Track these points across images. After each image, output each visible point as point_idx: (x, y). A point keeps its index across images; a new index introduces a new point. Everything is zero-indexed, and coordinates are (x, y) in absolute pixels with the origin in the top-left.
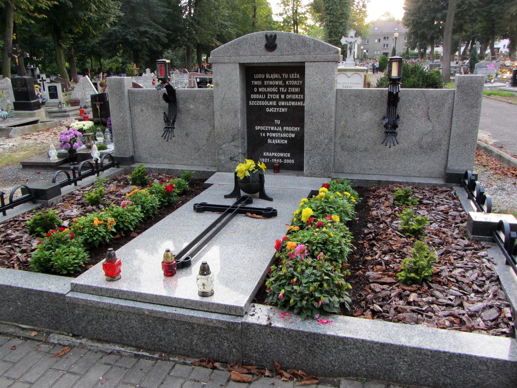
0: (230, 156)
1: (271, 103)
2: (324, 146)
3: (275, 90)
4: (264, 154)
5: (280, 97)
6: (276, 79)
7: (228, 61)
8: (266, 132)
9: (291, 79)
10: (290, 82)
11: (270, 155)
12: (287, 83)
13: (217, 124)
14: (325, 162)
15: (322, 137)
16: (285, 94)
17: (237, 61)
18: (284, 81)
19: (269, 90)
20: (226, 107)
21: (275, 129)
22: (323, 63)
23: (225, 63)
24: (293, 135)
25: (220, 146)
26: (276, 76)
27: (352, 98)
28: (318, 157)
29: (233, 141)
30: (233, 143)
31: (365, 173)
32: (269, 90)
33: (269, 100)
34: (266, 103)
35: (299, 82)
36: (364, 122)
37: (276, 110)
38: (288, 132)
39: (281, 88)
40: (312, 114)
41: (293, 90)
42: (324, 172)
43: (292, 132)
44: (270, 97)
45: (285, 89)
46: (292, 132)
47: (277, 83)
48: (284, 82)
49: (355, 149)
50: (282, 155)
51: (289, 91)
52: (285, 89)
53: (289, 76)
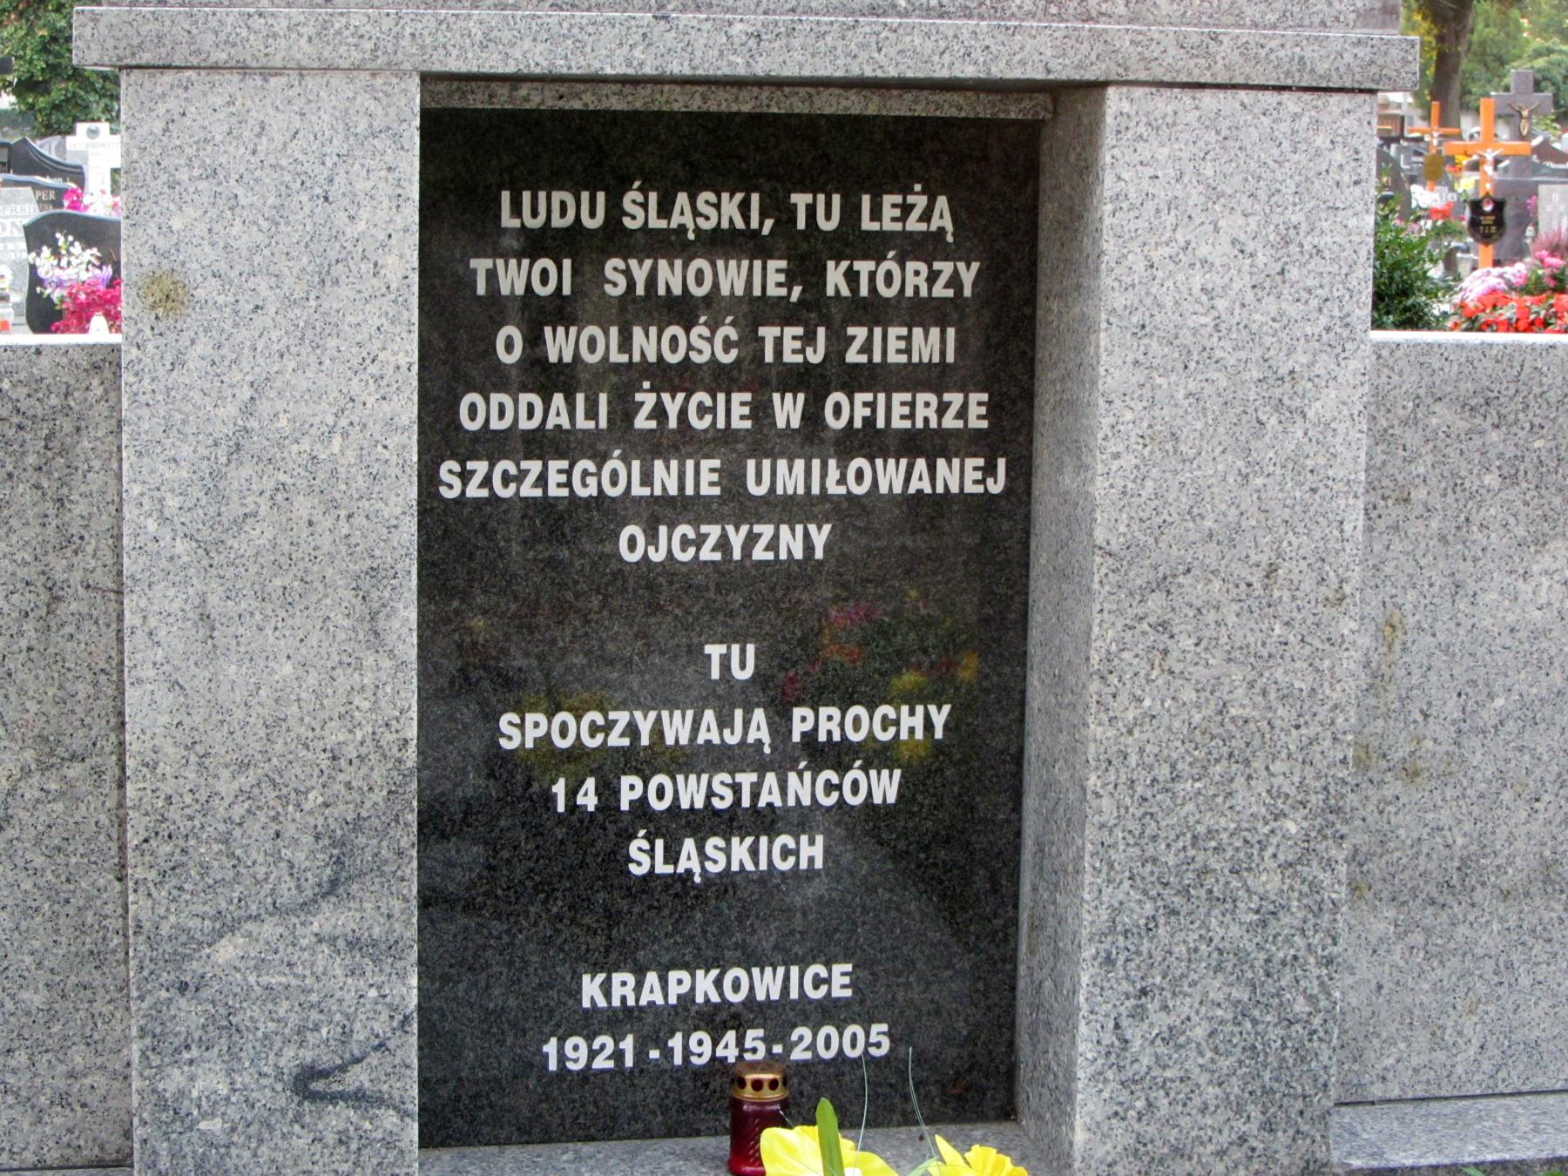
0: (291, 1058)
1: (666, 477)
2: (1269, 881)
3: (708, 344)
4: (591, 989)
5: (761, 412)
6: (720, 243)
7: (304, 51)
8: (607, 767)
9: (875, 246)
10: (864, 267)
11: (652, 992)
12: (835, 277)
13: (148, 710)
14: (1275, 1034)
15: (1249, 800)
16: (813, 383)
17: (413, 58)
18: (806, 260)
19: (646, 344)
20: (259, 534)
21: (710, 732)
22: (1270, 98)
23: (267, 72)
24: (885, 787)
25: (178, 960)
26: (724, 210)
27: (1443, 416)
28: (1216, 988)
29: (332, 888)
30: (331, 918)
31: (1540, 1081)
32: (646, 344)
33: (658, 446)
34: (618, 477)
35: (945, 268)
36: (1535, 635)
37: (723, 544)
38: (835, 755)
39: (768, 333)
40: (1163, 584)
41: (893, 345)
42: (1269, 1127)
43: (877, 756)
44: (659, 413)
45: (809, 339)
46: (877, 756)
47: (733, 277)
48: (807, 271)
49: (1461, 880)
50: (768, 984)
51: (853, 356)
52: (809, 339)
53: (851, 212)
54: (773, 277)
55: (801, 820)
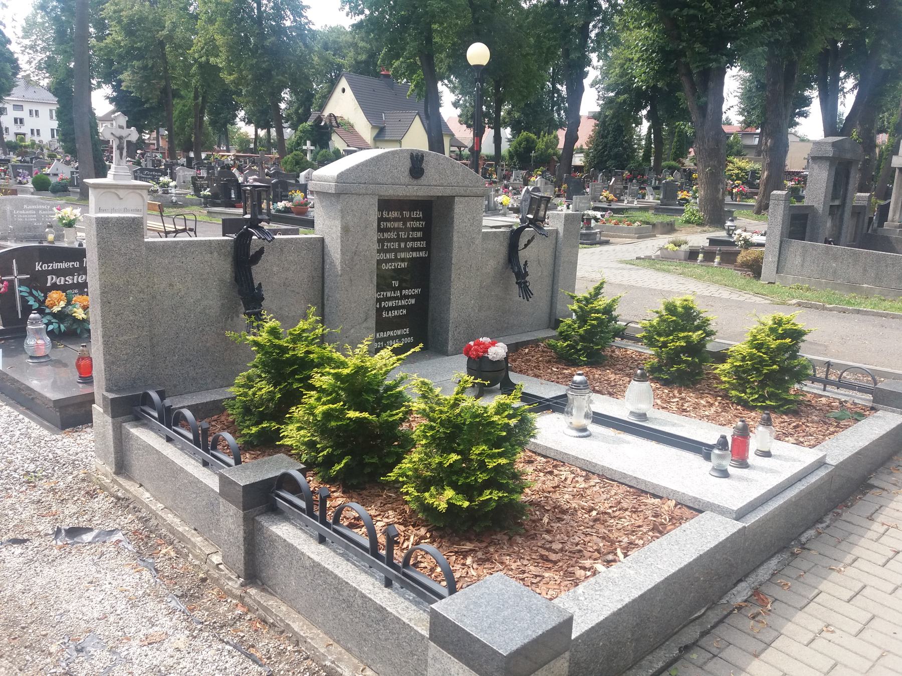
3: (393, 235)
5: (399, 245)
6: (395, 220)
20: (358, 266)
24: (413, 301)
26: (395, 214)
30: (365, 325)
46: (412, 297)
50: (399, 332)
54: (401, 224)
55: (402, 307)
